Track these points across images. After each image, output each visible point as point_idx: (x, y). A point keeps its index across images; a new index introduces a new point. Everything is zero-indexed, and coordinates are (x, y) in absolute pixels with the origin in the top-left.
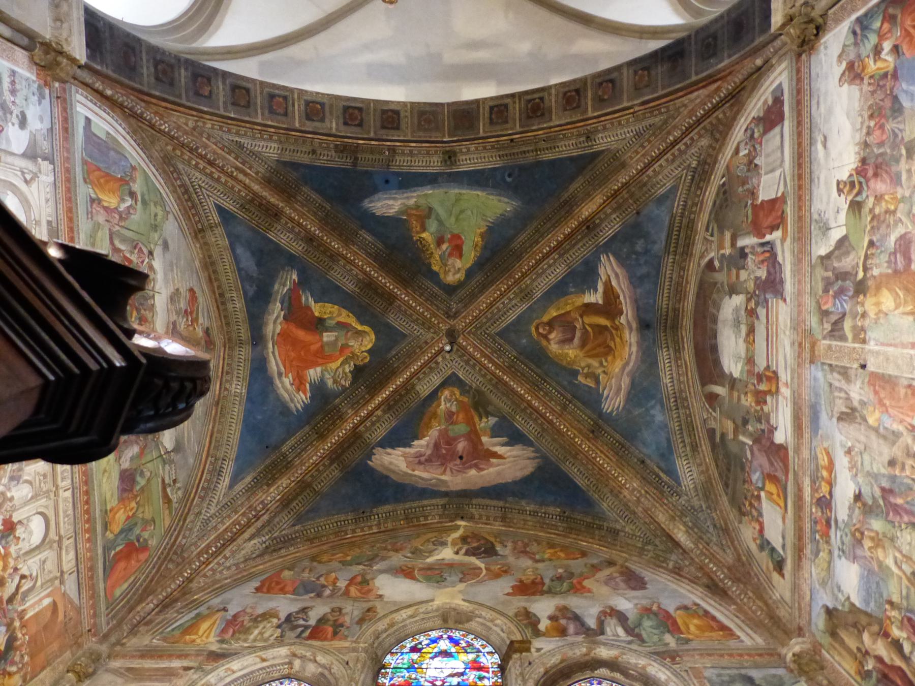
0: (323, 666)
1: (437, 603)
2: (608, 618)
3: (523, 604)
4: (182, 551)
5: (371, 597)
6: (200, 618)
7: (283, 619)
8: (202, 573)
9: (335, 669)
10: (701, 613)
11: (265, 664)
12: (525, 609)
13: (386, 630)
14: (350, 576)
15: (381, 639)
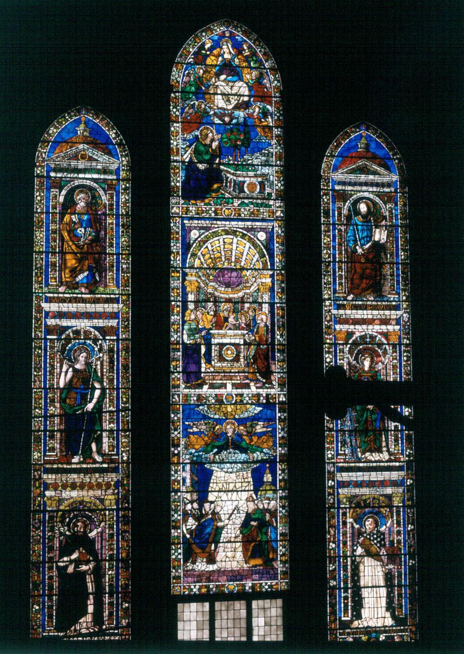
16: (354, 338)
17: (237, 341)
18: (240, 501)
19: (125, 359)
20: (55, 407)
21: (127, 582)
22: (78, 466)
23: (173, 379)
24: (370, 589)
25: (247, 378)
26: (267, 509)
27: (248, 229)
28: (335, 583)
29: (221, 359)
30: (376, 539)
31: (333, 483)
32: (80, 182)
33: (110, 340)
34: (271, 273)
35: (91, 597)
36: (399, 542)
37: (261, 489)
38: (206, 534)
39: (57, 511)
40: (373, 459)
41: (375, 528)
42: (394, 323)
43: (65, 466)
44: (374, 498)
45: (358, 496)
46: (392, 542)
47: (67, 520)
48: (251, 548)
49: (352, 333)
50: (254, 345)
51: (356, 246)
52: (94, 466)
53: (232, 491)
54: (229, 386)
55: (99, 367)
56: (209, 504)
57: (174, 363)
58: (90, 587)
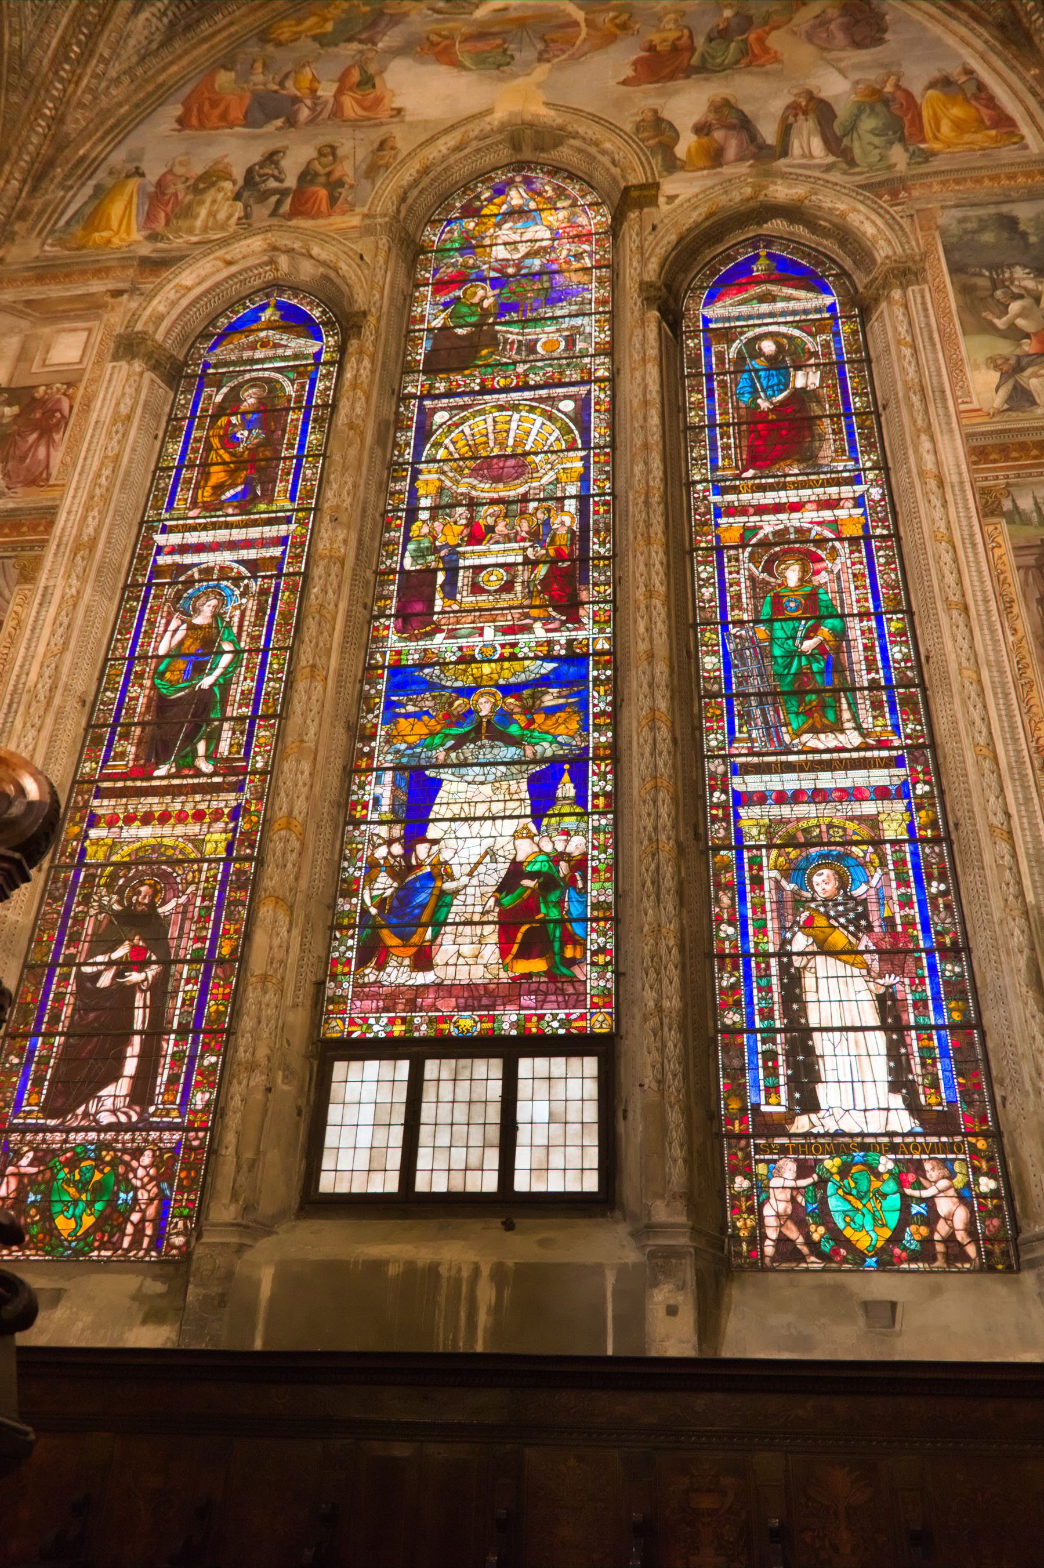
0: (324, 263)
1: (499, 115)
2: (801, 117)
3: (653, 102)
4: (23, 63)
5: (383, 114)
6: (101, 193)
7: (240, 182)
8: (74, 103)
9: (344, 267)
10: (971, 88)
11: (234, 269)
12: (655, 111)
13: (416, 183)
14: (338, 74)
15: (410, 201)
16: (761, 535)
17: (511, 559)
18: (499, 839)
19: (287, 603)
20: (141, 686)
21: (221, 1008)
22: (165, 783)
23: (377, 629)
24: (837, 1034)
25: (527, 616)
26: (562, 853)
27: (541, 400)
28: (737, 1018)
29: (476, 589)
30: (843, 914)
31: (723, 797)
32: (254, 374)
33: (264, 577)
34: (583, 453)
35: (137, 1040)
36: (908, 923)
37: (550, 812)
38: (415, 907)
39: (103, 866)
40: (821, 747)
41: (838, 889)
42: (849, 504)
43: (139, 784)
44: (830, 826)
45: (789, 821)
46: (889, 922)
47: (121, 882)
48: (520, 936)
49: (756, 529)
50: (545, 562)
51: (755, 399)
52: (196, 781)
53: (483, 818)
54: (489, 633)
55: (236, 619)
56: (427, 845)
57: (381, 603)
58: (139, 1019)
